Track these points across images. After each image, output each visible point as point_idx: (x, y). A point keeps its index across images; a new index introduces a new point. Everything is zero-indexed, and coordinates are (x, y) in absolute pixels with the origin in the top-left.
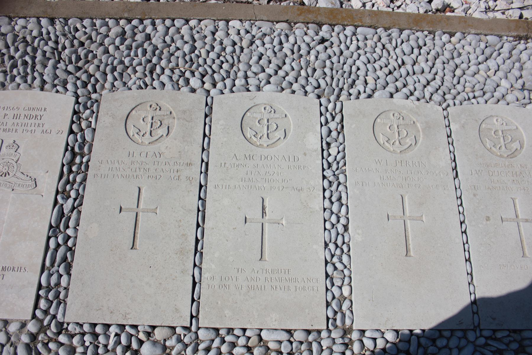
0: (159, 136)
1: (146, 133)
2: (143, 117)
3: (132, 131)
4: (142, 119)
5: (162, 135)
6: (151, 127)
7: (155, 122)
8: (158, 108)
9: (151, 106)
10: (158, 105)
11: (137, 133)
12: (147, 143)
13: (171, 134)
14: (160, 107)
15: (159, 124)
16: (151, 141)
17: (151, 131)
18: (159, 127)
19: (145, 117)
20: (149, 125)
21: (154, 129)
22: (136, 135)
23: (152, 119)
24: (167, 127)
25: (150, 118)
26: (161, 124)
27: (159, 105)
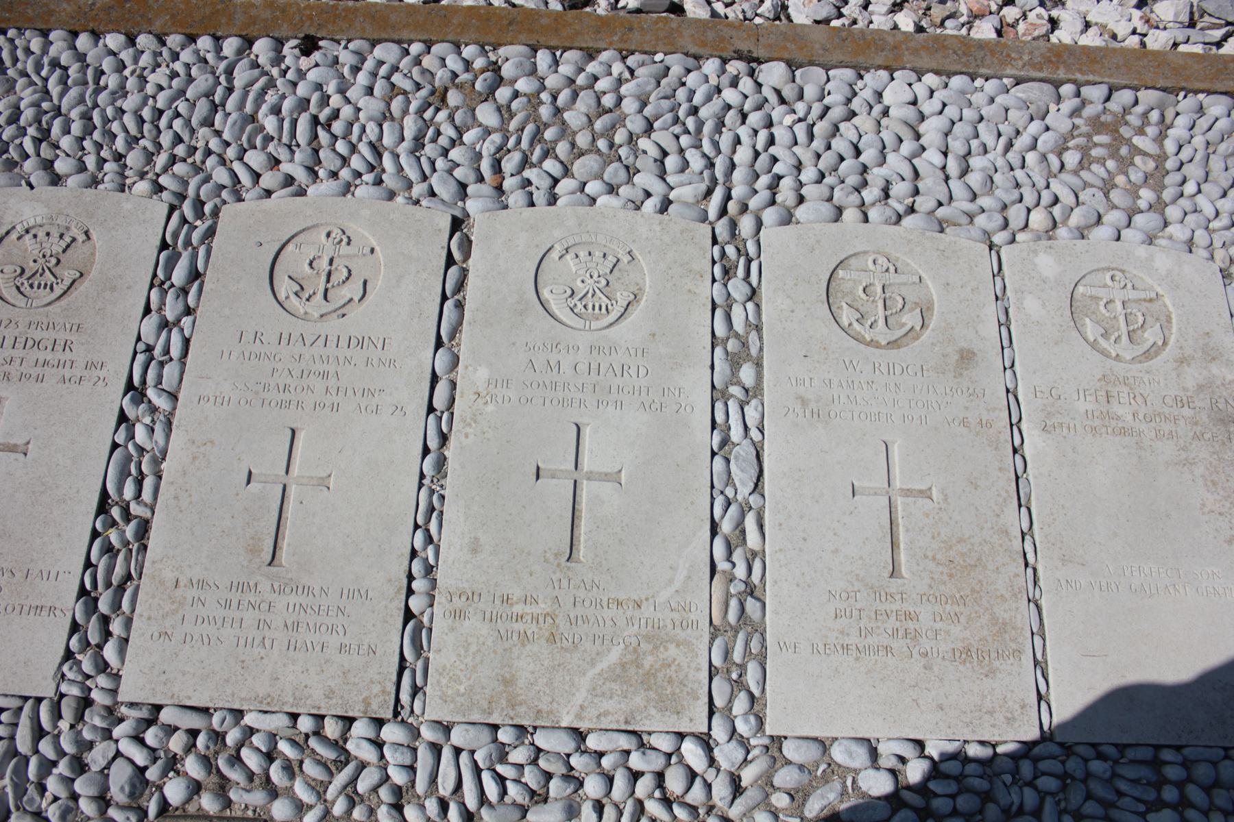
0: (347, 299)
1: (314, 293)
3: (285, 287)
4: (308, 261)
5: (351, 300)
6: (328, 281)
7: (336, 269)
8: (345, 240)
9: (328, 235)
10: (344, 233)
11: (296, 294)
12: (316, 315)
14: (349, 238)
15: (345, 273)
16: (324, 311)
17: (326, 290)
18: (344, 282)
19: (314, 259)
20: (324, 278)
21: (333, 286)
22: (293, 297)
23: (331, 261)
25: (326, 261)
27: (348, 233)
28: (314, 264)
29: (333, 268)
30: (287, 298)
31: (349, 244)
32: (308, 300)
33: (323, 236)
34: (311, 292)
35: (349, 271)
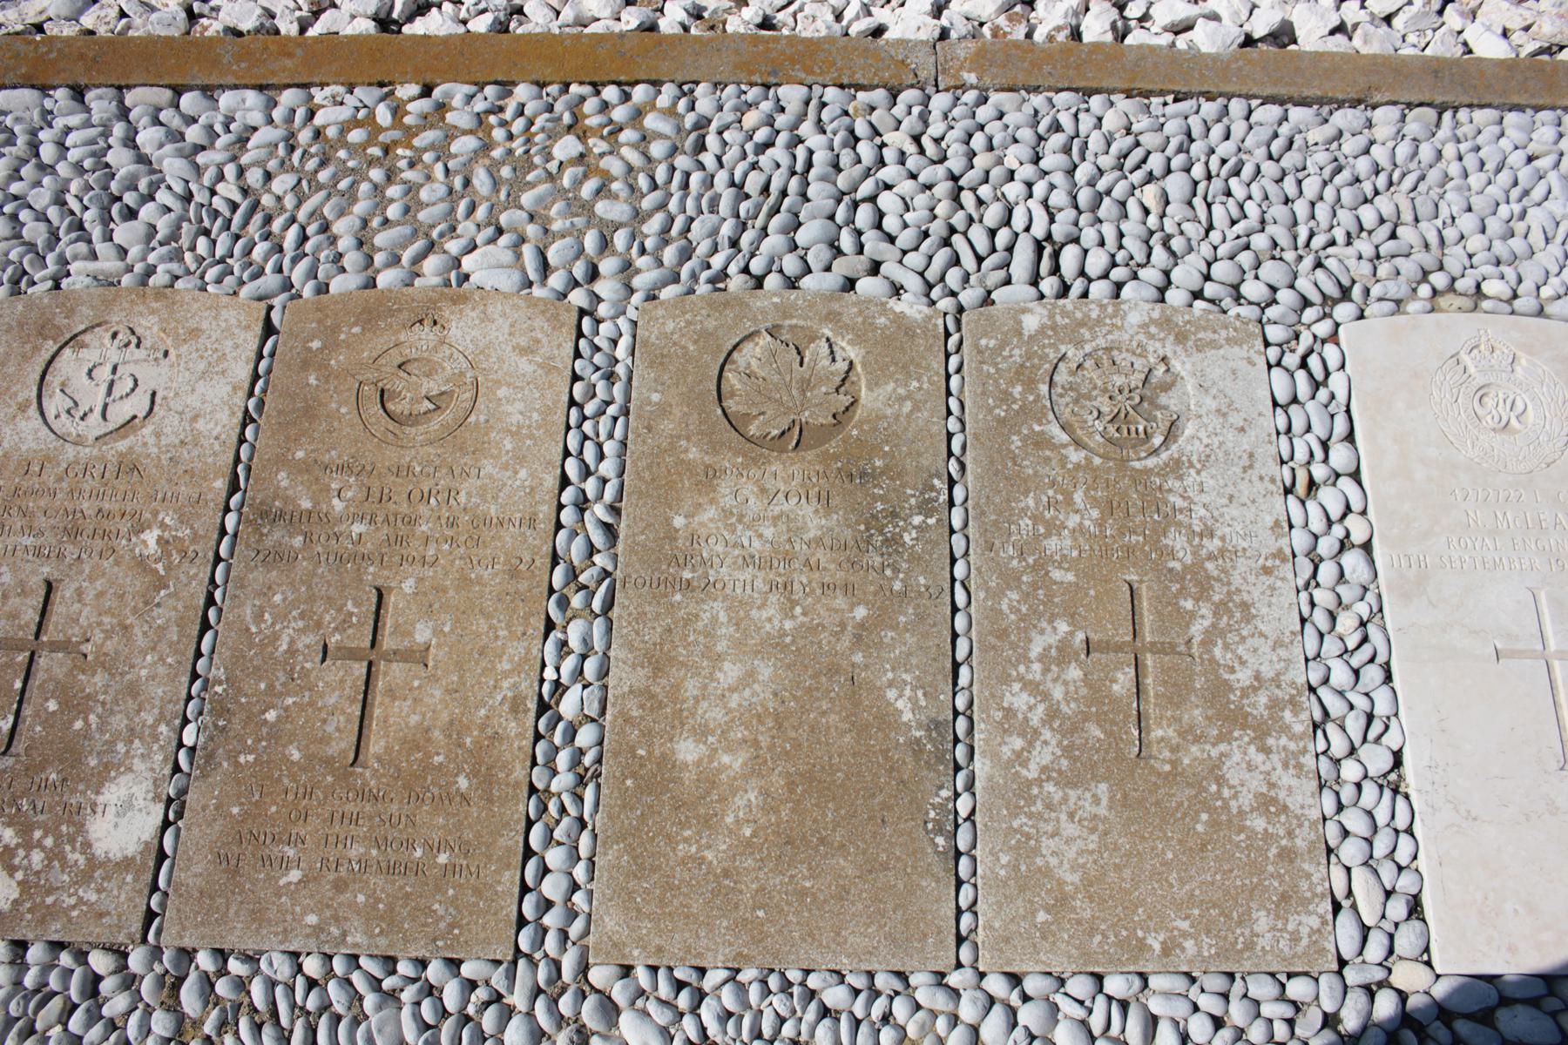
5: (135, 417)
8: (134, 341)
9: (114, 335)
10: (133, 333)
11: (68, 412)
15: (131, 384)
17: (106, 406)
20: (103, 388)
22: (64, 416)
25: (109, 368)
27: (139, 331)
29: (119, 374)
30: (57, 417)
31: (138, 346)
32: (82, 419)
35: (136, 381)
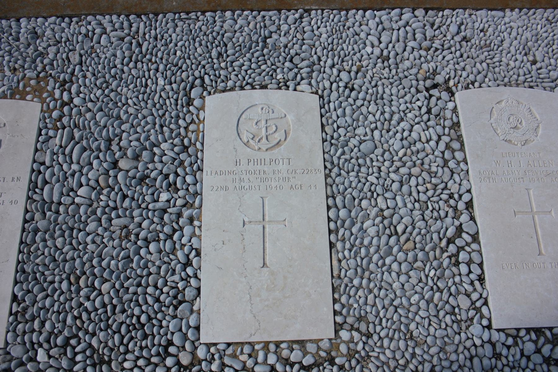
2: (256, 121)
4: (255, 122)
5: (280, 140)
6: (267, 132)
8: (271, 112)
9: (262, 109)
11: (252, 139)
12: (264, 149)
13: (288, 139)
17: (267, 136)
18: (275, 132)
20: (264, 130)
24: (283, 131)
25: (263, 122)
26: (277, 128)
27: (271, 107)
28: (258, 124)
29: (268, 125)
31: (273, 112)
33: (260, 110)
34: (260, 137)
